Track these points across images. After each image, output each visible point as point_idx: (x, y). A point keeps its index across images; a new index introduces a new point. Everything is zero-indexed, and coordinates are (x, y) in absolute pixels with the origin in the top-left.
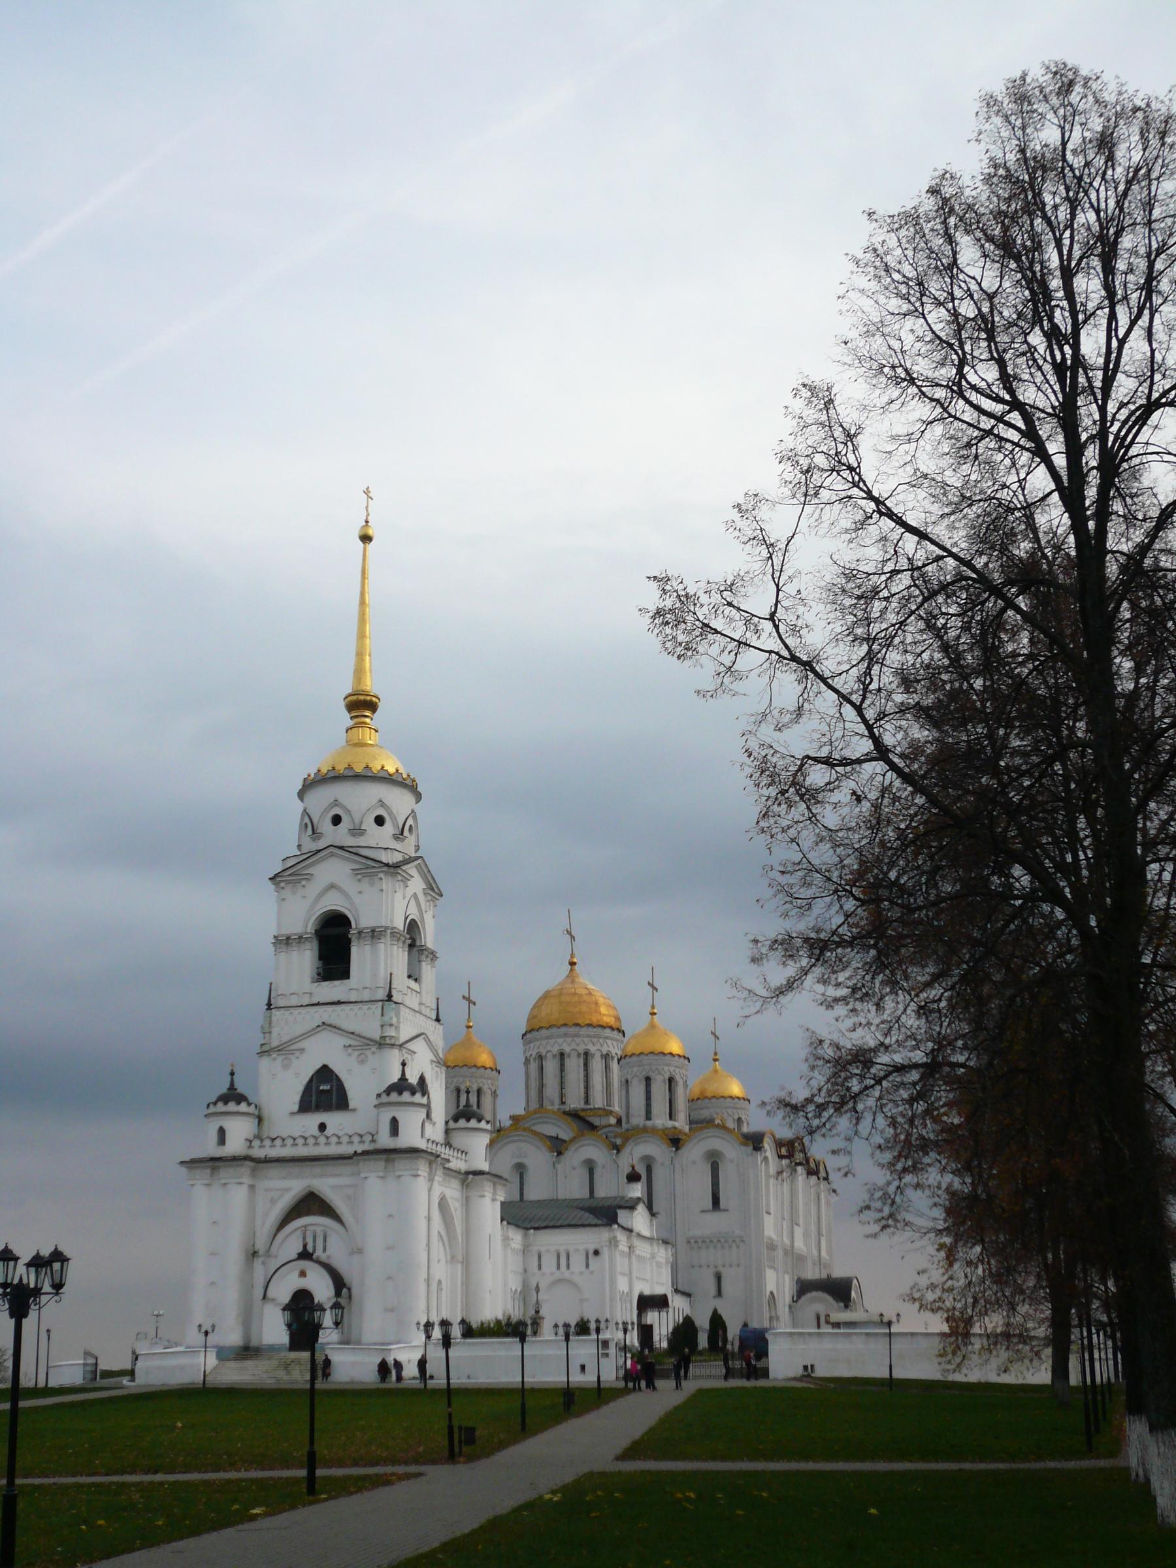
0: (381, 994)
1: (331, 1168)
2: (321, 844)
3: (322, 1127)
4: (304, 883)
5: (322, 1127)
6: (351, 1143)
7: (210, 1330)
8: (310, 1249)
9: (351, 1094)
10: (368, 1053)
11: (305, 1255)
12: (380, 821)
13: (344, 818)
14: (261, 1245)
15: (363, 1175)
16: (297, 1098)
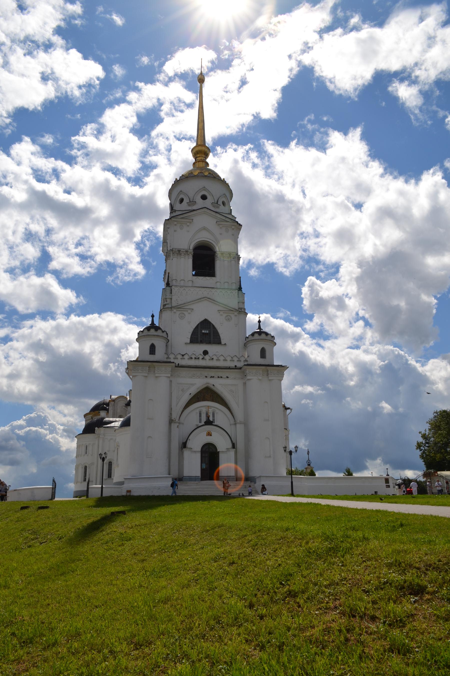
0: (235, 286)
1: (224, 373)
2: (194, 207)
3: (205, 353)
4: (188, 224)
5: (205, 353)
6: (232, 360)
7: (293, 450)
8: (211, 419)
9: (222, 336)
10: (233, 316)
11: (209, 422)
12: (224, 203)
13: (209, 197)
14: (175, 416)
15: (248, 378)
16: (189, 336)
